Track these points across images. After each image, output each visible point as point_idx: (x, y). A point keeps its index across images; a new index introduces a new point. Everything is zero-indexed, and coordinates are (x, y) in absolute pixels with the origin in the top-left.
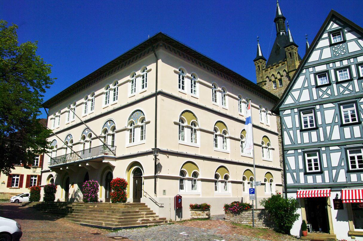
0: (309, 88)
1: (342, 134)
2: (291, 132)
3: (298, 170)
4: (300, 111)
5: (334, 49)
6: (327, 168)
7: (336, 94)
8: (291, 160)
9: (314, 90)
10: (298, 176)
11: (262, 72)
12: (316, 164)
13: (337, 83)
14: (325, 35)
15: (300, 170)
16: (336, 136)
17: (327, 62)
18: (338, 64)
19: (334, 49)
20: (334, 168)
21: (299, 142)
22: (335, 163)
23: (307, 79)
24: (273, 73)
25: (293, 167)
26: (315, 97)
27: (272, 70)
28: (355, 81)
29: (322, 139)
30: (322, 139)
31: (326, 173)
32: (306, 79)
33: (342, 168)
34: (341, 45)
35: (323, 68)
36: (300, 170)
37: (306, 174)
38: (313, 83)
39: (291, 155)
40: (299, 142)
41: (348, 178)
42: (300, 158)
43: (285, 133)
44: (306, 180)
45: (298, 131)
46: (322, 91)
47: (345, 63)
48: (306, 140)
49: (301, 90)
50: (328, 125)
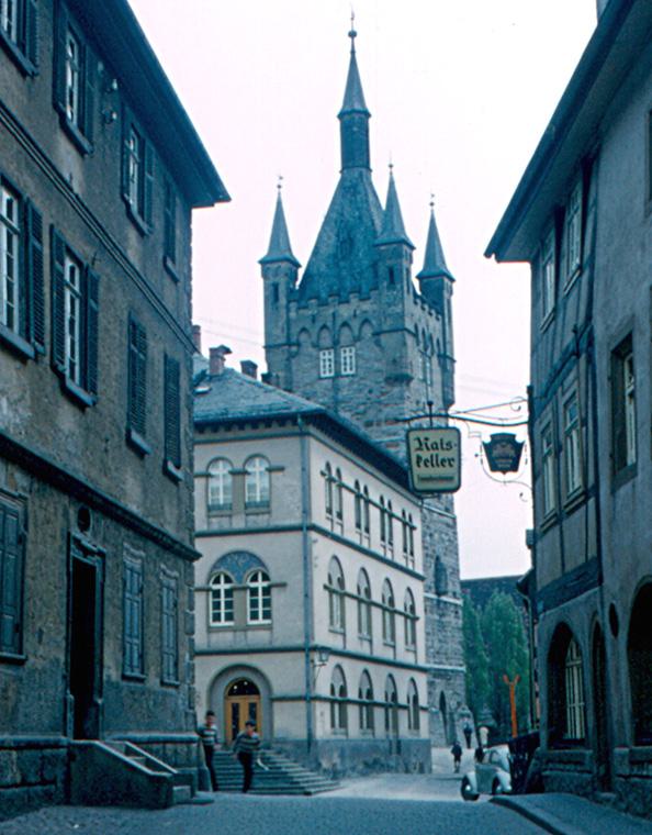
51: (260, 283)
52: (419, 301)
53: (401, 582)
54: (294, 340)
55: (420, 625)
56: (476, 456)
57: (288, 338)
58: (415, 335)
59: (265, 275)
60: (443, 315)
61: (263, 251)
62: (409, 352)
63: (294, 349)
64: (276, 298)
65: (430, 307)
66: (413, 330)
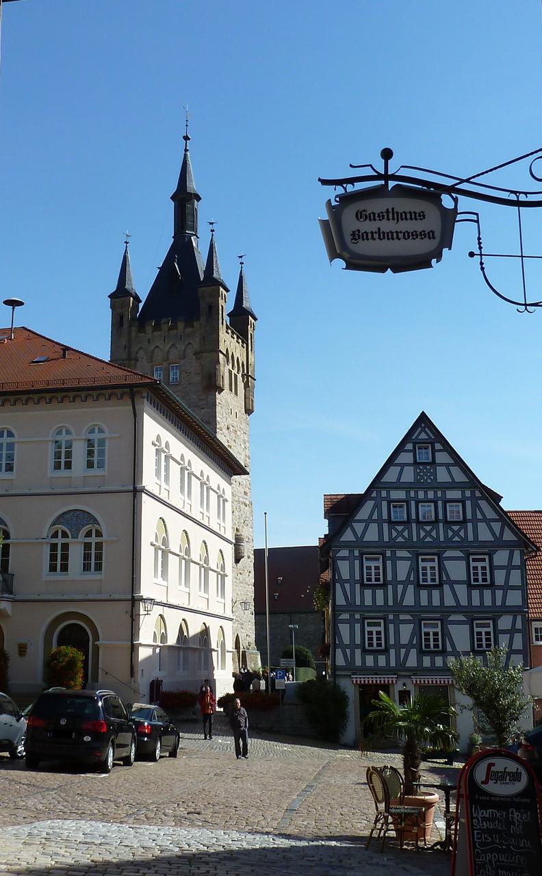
0: (380, 522)
1: (417, 597)
2: (347, 586)
3: (353, 646)
4: (362, 554)
6: (394, 646)
7: (415, 540)
9: (386, 526)
10: (353, 654)
11: (129, 333)
12: (379, 639)
13: (418, 522)
14: (409, 446)
15: (357, 646)
16: (409, 600)
17: (407, 487)
18: (421, 495)
20: (403, 646)
21: (358, 602)
22: (405, 639)
23: (377, 506)
24: (157, 344)
25: (346, 641)
26: (386, 539)
29: (391, 603)
30: (391, 603)
31: (392, 652)
32: (375, 506)
33: (413, 646)
34: (428, 467)
35: (401, 495)
36: (357, 646)
37: (365, 652)
38: (385, 516)
39: (344, 621)
40: (358, 602)
41: (420, 661)
42: (358, 626)
43: (338, 585)
45: (358, 586)
47: (431, 495)
48: (368, 602)
50: (401, 582)
51: (108, 313)
53: (215, 544)
56: (472, 254)
57: (129, 356)
58: (226, 356)
59: (113, 307)
61: (113, 288)
62: (221, 368)
63: (133, 362)
64: (121, 324)
65: (238, 338)
66: (225, 353)
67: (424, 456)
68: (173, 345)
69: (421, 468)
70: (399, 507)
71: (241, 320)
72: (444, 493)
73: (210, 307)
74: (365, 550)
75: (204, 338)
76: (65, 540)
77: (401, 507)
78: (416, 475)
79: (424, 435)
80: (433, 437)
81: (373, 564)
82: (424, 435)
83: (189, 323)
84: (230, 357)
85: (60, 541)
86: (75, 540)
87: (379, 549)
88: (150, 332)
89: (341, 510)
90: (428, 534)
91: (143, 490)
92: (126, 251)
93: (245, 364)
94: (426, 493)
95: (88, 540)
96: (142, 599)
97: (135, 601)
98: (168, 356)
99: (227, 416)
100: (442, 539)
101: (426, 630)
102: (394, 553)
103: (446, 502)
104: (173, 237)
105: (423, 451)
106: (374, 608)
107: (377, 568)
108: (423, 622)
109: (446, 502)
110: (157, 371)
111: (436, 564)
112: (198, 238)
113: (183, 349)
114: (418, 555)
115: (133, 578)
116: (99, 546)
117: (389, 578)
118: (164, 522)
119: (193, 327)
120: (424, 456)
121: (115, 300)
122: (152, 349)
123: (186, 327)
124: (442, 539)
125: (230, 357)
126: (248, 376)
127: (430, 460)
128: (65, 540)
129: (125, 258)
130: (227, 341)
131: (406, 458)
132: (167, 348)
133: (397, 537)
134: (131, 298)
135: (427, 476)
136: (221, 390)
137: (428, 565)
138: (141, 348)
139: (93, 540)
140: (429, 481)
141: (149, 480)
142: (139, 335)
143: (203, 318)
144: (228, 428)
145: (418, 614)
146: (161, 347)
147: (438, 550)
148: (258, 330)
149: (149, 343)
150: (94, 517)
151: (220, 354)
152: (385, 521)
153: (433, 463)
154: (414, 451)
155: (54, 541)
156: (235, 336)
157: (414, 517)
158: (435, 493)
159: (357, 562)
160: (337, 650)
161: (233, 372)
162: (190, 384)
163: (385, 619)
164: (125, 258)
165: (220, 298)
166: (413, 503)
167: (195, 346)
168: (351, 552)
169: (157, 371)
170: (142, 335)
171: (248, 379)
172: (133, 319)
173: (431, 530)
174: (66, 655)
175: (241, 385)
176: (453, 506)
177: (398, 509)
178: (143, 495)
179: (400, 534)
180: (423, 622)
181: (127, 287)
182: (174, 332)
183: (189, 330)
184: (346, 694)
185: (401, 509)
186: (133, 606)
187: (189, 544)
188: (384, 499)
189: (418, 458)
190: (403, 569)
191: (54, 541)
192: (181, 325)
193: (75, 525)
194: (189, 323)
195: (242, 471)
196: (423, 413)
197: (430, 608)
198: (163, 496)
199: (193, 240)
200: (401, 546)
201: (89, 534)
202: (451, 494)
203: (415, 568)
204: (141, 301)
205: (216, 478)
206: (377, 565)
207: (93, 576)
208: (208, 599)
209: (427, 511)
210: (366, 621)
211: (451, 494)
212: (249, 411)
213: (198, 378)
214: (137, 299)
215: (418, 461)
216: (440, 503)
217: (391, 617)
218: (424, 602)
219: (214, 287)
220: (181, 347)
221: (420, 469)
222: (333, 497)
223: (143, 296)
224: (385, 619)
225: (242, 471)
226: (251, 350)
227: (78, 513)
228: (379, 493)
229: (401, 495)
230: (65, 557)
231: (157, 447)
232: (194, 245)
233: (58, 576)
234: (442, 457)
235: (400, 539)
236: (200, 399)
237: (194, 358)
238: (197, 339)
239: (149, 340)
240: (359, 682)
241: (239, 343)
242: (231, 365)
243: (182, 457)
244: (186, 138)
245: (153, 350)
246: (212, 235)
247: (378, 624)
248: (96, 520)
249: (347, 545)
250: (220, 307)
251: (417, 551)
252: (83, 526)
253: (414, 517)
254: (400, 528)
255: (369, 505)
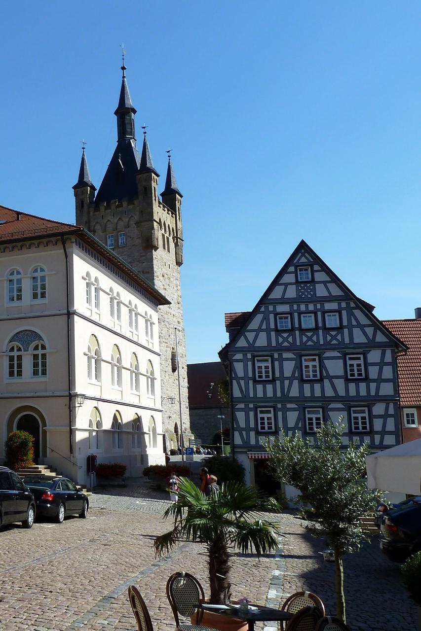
0: (268, 330)
2: (242, 382)
3: (248, 429)
4: (254, 357)
5: (300, 288)
7: (298, 344)
8: (240, 416)
9: (273, 334)
10: (248, 436)
11: (89, 212)
12: (269, 423)
14: (292, 269)
15: (252, 429)
16: (294, 392)
17: (290, 302)
18: (303, 308)
19: (300, 288)
21: (251, 395)
23: (266, 319)
24: (109, 219)
26: (274, 344)
27: (107, 211)
28: (321, 331)
29: (279, 394)
30: (279, 394)
34: (308, 285)
35: (285, 308)
36: (252, 429)
37: (258, 433)
38: (272, 326)
39: (240, 410)
40: (251, 395)
42: (252, 414)
44: (257, 441)
45: (251, 382)
46: (282, 337)
47: (311, 307)
49: (259, 330)
50: (287, 378)
52: (161, 206)
54: (92, 228)
55: (157, 383)
58: (160, 223)
59: (75, 195)
60: (176, 213)
61: (75, 181)
62: (156, 232)
64: (83, 207)
65: (168, 210)
67: (305, 276)
68: (120, 218)
69: (302, 285)
70: (285, 318)
71: (170, 198)
72: (322, 305)
73: (146, 189)
74: (256, 353)
75: (142, 211)
76: (19, 353)
77: (286, 318)
78: (298, 291)
79: (304, 259)
80: (312, 261)
81: (263, 365)
82: (304, 259)
83: (130, 202)
84: (163, 225)
85: (15, 353)
86: (26, 353)
87: (268, 352)
88: (103, 210)
89: (237, 324)
90: (310, 339)
91: (75, 313)
92: (83, 155)
93: (175, 229)
94: (307, 306)
95: (36, 352)
96: (76, 395)
97: (71, 397)
98: (117, 227)
99: (162, 267)
100: (322, 342)
101: (310, 416)
102: (280, 355)
103: (324, 312)
104: (117, 142)
105: (304, 272)
106: (265, 399)
107: (267, 367)
108: (307, 410)
109: (324, 312)
110: (109, 238)
111: (317, 363)
112: (136, 140)
113: (127, 220)
114: (301, 356)
115: (69, 379)
116: (44, 356)
117: (277, 375)
118: (96, 338)
119: (134, 204)
120: (305, 276)
121: (77, 190)
122: (105, 222)
123: (128, 205)
124: (322, 342)
125: (163, 225)
126: (177, 238)
127: (310, 279)
128: (19, 353)
129: (83, 160)
130: (159, 213)
131: (289, 278)
132: (116, 221)
133: (282, 343)
134: (89, 188)
135: (307, 292)
136: (156, 248)
137: (310, 365)
138: (97, 223)
139: (40, 352)
140: (309, 296)
141: (80, 304)
142: (96, 213)
143: (141, 198)
144: (163, 276)
145: (303, 404)
146: (112, 220)
147: (319, 352)
148: (183, 204)
149: (103, 218)
150: (39, 335)
151: (154, 222)
152: (272, 330)
153: (313, 281)
154: (296, 273)
155: (12, 354)
156: (166, 209)
157: (297, 325)
158: (315, 306)
159: (250, 364)
160: (235, 432)
161: (166, 235)
162: (133, 245)
163: (275, 408)
164: (83, 160)
165: (153, 181)
166: (296, 315)
167: (136, 218)
168: (245, 355)
169: (109, 238)
170: (98, 213)
171: (177, 240)
172: (91, 202)
173: (312, 336)
174: (19, 437)
175: (172, 245)
176: (330, 316)
177: (283, 320)
178: (75, 316)
179: (285, 339)
180: (307, 410)
181: (85, 180)
182: (120, 209)
183: (131, 207)
184: (243, 467)
185: (286, 320)
186: (70, 400)
187: (120, 355)
188: (271, 312)
189: (299, 278)
190: (289, 368)
191: (12, 354)
192: (125, 204)
193: (26, 342)
194: (130, 202)
195: (166, 302)
196: (303, 241)
197: (313, 398)
198: (95, 318)
199: (132, 142)
200: (287, 349)
201: (36, 348)
202: (328, 306)
203: (299, 366)
204: (96, 190)
205: (143, 307)
206: (266, 365)
207: (40, 379)
208: (122, 392)
209: (308, 322)
210: (259, 410)
211: (328, 306)
212: (179, 263)
213: (140, 241)
214: (93, 188)
215: (299, 280)
216: (319, 314)
217: (279, 406)
218: (307, 393)
219: (147, 174)
220: (126, 219)
221: (301, 287)
222: (232, 315)
223: (98, 186)
224: (275, 408)
225: (166, 302)
226: (179, 219)
227: (28, 332)
228: (267, 308)
229: (285, 308)
230: (20, 366)
231: (110, 296)
232: (133, 146)
233: (16, 380)
234: (320, 276)
235: (286, 344)
236: (141, 256)
237: (136, 227)
238: (137, 213)
239: (103, 216)
240: (253, 457)
241: (169, 214)
242: (163, 230)
243: (130, 302)
244: (123, 68)
245: (106, 224)
246: (145, 136)
247: (269, 412)
248: (41, 337)
249: (242, 350)
250: (153, 188)
251: (300, 352)
252: (32, 342)
253: (297, 325)
254: (285, 335)
255: (259, 318)
